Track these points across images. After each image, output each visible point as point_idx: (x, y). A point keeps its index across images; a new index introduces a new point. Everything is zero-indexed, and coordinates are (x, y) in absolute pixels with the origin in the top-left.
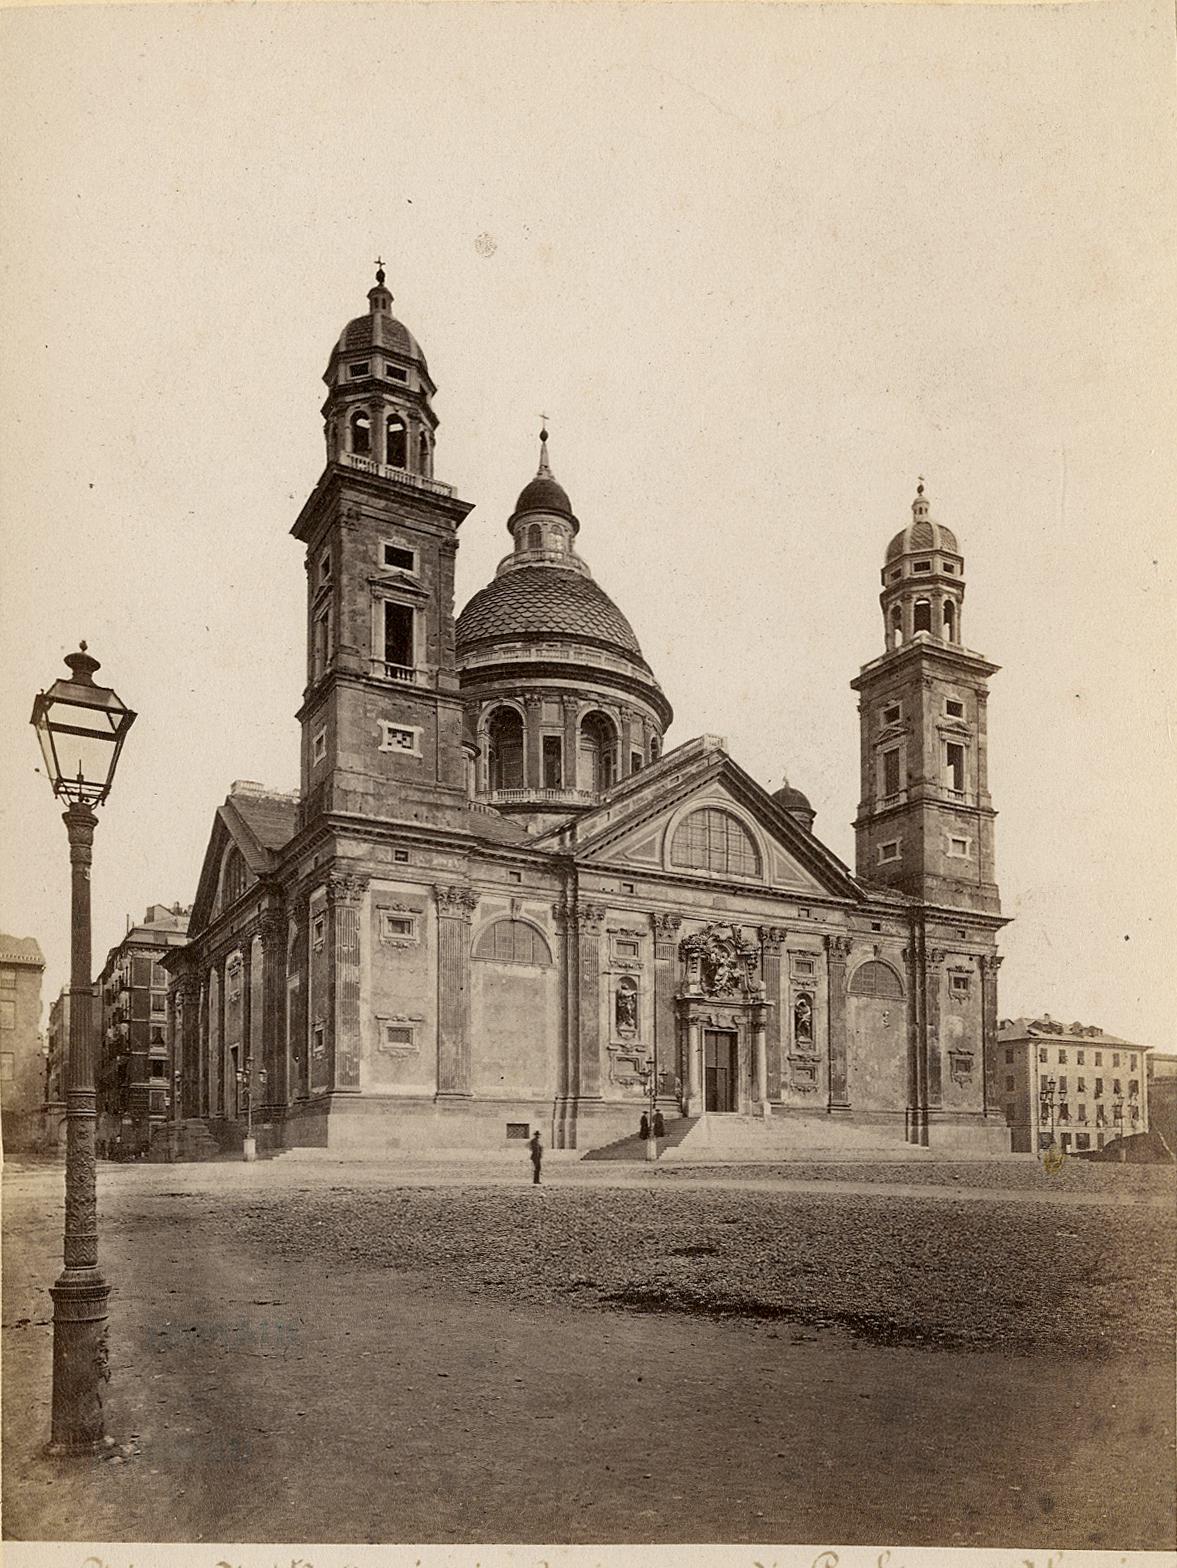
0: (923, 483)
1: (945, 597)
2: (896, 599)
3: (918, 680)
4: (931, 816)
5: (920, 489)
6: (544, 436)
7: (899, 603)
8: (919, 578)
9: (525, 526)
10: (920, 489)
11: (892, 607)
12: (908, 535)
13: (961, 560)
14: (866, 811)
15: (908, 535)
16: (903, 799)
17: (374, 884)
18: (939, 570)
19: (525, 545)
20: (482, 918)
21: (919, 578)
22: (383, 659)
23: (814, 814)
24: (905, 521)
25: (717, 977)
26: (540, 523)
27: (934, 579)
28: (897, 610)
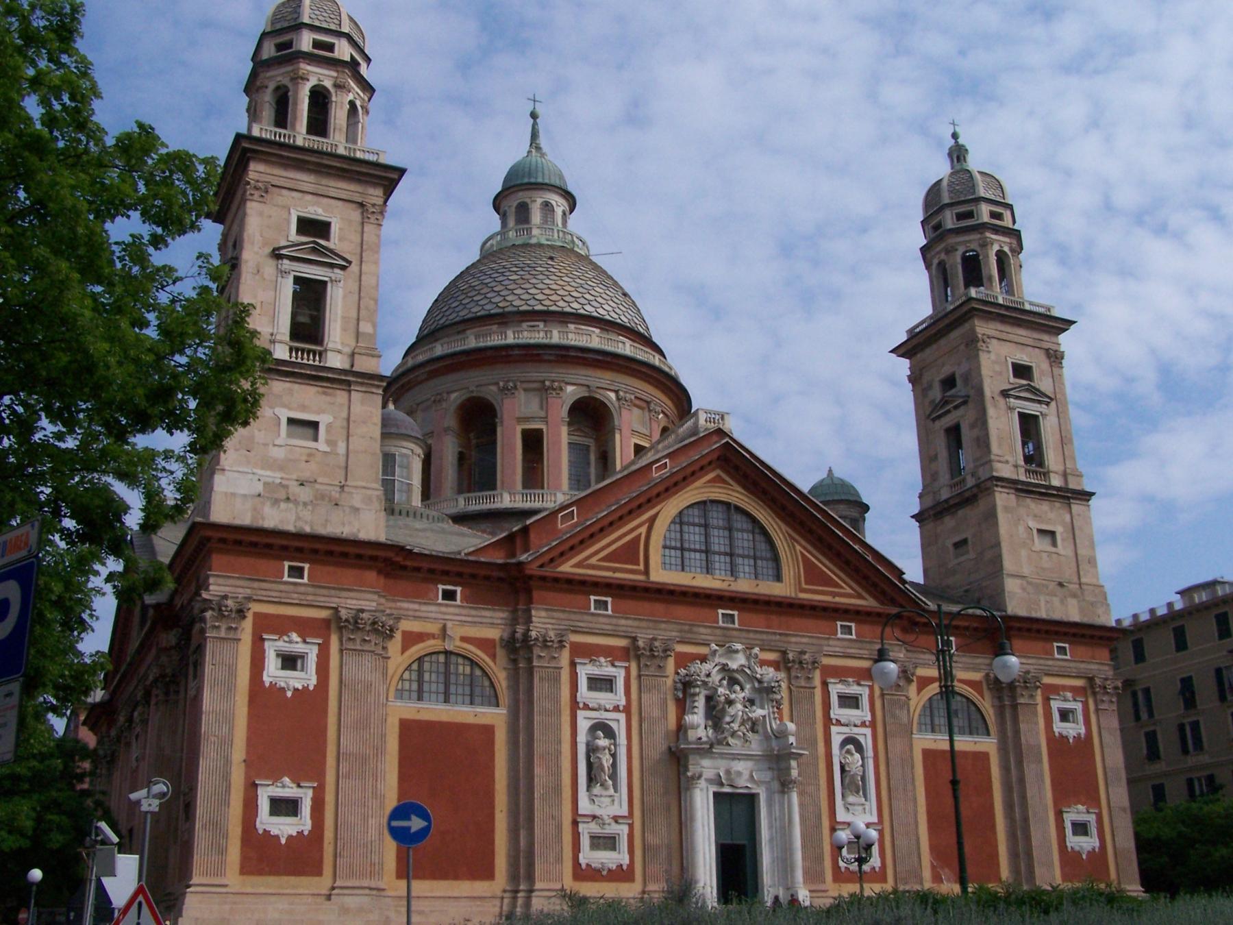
0: (958, 129)
1: (996, 247)
2: (938, 253)
3: (972, 343)
4: (1003, 499)
6: (534, 116)
7: (943, 256)
8: (965, 232)
9: (511, 204)
11: (935, 261)
12: (945, 183)
13: (1010, 207)
14: (929, 502)
15: (945, 183)
16: (970, 482)
17: (256, 608)
18: (986, 218)
19: (511, 223)
20: (404, 649)
21: (965, 232)
22: (287, 338)
23: (866, 508)
24: (941, 169)
25: (728, 719)
26: (528, 201)
27: (983, 227)
28: (942, 264)
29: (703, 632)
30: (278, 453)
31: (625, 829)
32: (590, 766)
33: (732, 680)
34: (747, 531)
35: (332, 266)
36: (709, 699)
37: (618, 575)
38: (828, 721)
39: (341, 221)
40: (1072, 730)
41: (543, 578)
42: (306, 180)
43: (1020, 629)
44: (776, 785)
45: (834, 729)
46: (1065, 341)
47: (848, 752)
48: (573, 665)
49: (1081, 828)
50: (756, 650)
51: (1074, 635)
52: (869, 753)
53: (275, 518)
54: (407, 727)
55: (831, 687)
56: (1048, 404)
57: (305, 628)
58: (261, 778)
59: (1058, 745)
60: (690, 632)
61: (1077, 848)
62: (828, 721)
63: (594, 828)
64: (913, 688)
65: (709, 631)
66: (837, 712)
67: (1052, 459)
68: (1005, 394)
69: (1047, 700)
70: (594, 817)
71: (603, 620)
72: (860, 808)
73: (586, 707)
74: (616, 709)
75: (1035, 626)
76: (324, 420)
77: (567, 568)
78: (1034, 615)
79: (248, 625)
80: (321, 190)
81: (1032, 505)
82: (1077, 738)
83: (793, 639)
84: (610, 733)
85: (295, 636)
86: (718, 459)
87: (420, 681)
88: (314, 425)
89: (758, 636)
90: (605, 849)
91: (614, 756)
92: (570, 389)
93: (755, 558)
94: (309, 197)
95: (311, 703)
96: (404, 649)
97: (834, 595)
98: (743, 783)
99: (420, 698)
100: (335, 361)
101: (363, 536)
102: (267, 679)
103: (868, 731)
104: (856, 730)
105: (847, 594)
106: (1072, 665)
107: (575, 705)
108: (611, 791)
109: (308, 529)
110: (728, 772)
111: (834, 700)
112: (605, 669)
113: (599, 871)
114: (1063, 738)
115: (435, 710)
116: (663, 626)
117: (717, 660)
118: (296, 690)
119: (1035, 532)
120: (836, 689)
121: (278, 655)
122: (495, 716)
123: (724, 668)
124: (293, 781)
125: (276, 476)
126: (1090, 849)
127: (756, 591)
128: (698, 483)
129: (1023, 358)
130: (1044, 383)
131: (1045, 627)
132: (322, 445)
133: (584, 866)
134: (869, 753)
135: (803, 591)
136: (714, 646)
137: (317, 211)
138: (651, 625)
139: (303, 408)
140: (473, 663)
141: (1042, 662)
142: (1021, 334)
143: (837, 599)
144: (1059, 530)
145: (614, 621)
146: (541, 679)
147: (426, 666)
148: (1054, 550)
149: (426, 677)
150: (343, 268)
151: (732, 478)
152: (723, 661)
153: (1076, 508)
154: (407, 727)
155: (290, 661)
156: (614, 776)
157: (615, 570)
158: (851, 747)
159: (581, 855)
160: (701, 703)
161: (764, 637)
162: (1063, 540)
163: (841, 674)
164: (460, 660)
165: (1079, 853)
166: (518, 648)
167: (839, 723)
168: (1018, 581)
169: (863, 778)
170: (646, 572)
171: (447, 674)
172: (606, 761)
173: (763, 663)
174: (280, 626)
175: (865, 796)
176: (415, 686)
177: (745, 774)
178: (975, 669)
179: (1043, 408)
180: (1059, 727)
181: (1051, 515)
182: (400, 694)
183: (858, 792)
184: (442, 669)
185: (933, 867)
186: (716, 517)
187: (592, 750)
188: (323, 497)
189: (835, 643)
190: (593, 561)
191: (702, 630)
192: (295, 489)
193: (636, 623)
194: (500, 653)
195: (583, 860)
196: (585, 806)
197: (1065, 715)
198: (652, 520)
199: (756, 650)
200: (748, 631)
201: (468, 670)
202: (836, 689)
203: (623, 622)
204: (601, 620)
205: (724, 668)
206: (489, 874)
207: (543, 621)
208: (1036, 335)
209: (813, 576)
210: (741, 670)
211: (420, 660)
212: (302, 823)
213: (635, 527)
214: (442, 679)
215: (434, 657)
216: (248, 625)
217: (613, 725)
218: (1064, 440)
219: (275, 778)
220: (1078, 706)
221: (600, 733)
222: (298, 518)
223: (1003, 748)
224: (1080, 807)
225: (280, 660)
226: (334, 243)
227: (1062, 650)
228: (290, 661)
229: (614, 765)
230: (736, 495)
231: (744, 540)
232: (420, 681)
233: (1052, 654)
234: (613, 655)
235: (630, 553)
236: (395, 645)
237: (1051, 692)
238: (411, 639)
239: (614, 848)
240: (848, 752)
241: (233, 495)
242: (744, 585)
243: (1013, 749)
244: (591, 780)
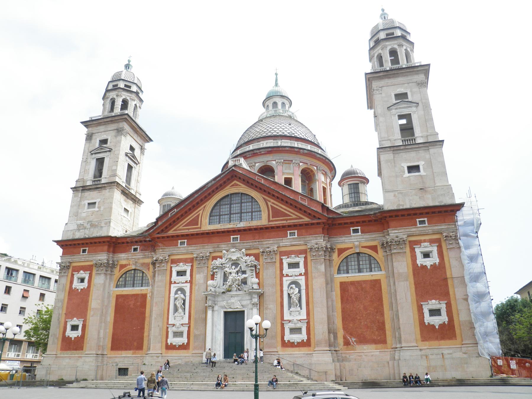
6: (276, 74)
20: (120, 271)
29: (223, 246)
30: (84, 215)
31: (187, 329)
32: (175, 305)
33: (235, 264)
34: (249, 202)
35: (106, 152)
37: (190, 231)
38: (282, 275)
39: (109, 136)
40: (428, 262)
41: (158, 238)
42: (102, 128)
43: (390, 217)
44: (250, 306)
45: (285, 279)
47: (291, 288)
48: (171, 267)
49: (435, 312)
50: (243, 250)
51: (427, 213)
52: (303, 287)
53: (78, 235)
55: (284, 261)
56: (417, 107)
57: (84, 268)
58: (69, 318)
59: (419, 272)
60: (218, 247)
61: (432, 323)
62: (282, 275)
63: (174, 329)
64: (335, 255)
65: (226, 246)
66: (286, 270)
69: (413, 250)
70: (174, 325)
71: (182, 249)
72: (298, 313)
73: (175, 283)
74: (186, 282)
75: (400, 213)
76: (97, 201)
77: (171, 232)
78: (401, 207)
79: (70, 270)
80: (106, 129)
81: (404, 155)
82: (434, 266)
83: (265, 243)
85: (82, 272)
86: (232, 177)
87: (125, 281)
88: (95, 203)
89: (248, 244)
90: (179, 337)
91: (184, 301)
92: (257, 164)
93: (252, 212)
94: (103, 133)
95: (86, 292)
96: (120, 271)
97: (287, 220)
99: (125, 287)
100: (103, 181)
101: (103, 235)
102: (74, 287)
103: (303, 278)
104: (296, 278)
105: (295, 217)
106: (428, 228)
107: (171, 283)
108: (182, 314)
109: (87, 237)
110: (227, 303)
111: (285, 266)
112: (182, 267)
113: (175, 346)
114: (424, 267)
115: (128, 290)
116: (206, 247)
117: (226, 257)
118: (81, 289)
119: (406, 169)
120: (286, 261)
121: (78, 279)
124: (78, 319)
125: (81, 222)
126: (441, 323)
127: (249, 225)
128: (228, 187)
129: (400, 90)
131: (406, 213)
133: (169, 344)
135: (272, 221)
136: (224, 251)
137: (104, 137)
138: (201, 247)
139: (93, 199)
140: (143, 273)
141: (407, 230)
142: (400, 80)
143: (289, 221)
144: (421, 164)
145: (187, 248)
146: (158, 274)
147: (128, 275)
148: (417, 174)
149: (127, 279)
150: (110, 151)
151: (242, 183)
152: (229, 257)
153: (432, 150)
155: (82, 280)
157: (188, 229)
158: (294, 286)
159: (168, 340)
161: (251, 244)
162: (424, 168)
163: (288, 254)
164: (139, 272)
165: (433, 326)
166: (154, 264)
167: (287, 275)
168: (392, 194)
170: (200, 228)
171: (134, 277)
173: (247, 255)
174: (77, 269)
175: (300, 306)
176: (123, 283)
178: (375, 240)
179: (414, 109)
180: (420, 261)
182: (117, 286)
183: (297, 306)
184: (132, 276)
185: (345, 338)
187: (176, 299)
188: (93, 225)
189: (286, 241)
190: (181, 228)
191: (223, 246)
192: (85, 225)
193: (195, 248)
194: (151, 266)
195: (169, 342)
197: (426, 255)
198: (204, 207)
199: (243, 250)
200: (244, 243)
201: (141, 275)
202: (286, 261)
203: (190, 248)
204: (183, 249)
207: (161, 254)
208: (409, 78)
209: (276, 213)
210: (238, 259)
211: (125, 273)
213: (199, 211)
214: (132, 279)
215: (130, 272)
216: (70, 270)
217: (184, 288)
218: (428, 119)
219: (72, 318)
220: (434, 249)
221: (179, 292)
222: (85, 234)
223: (388, 277)
224: (434, 301)
225: (79, 280)
226: (109, 144)
227: (422, 222)
229: (184, 304)
230: (243, 189)
231: (247, 206)
232: (125, 281)
233: (416, 225)
234: (185, 261)
235: (195, 222)
237: (413, 244)
238: (122, 266)
239: (182, 337)
240: (291, 288)
241: (68, 231)
242: (242, 225)
243: (391, 274)
244: (176, 310)
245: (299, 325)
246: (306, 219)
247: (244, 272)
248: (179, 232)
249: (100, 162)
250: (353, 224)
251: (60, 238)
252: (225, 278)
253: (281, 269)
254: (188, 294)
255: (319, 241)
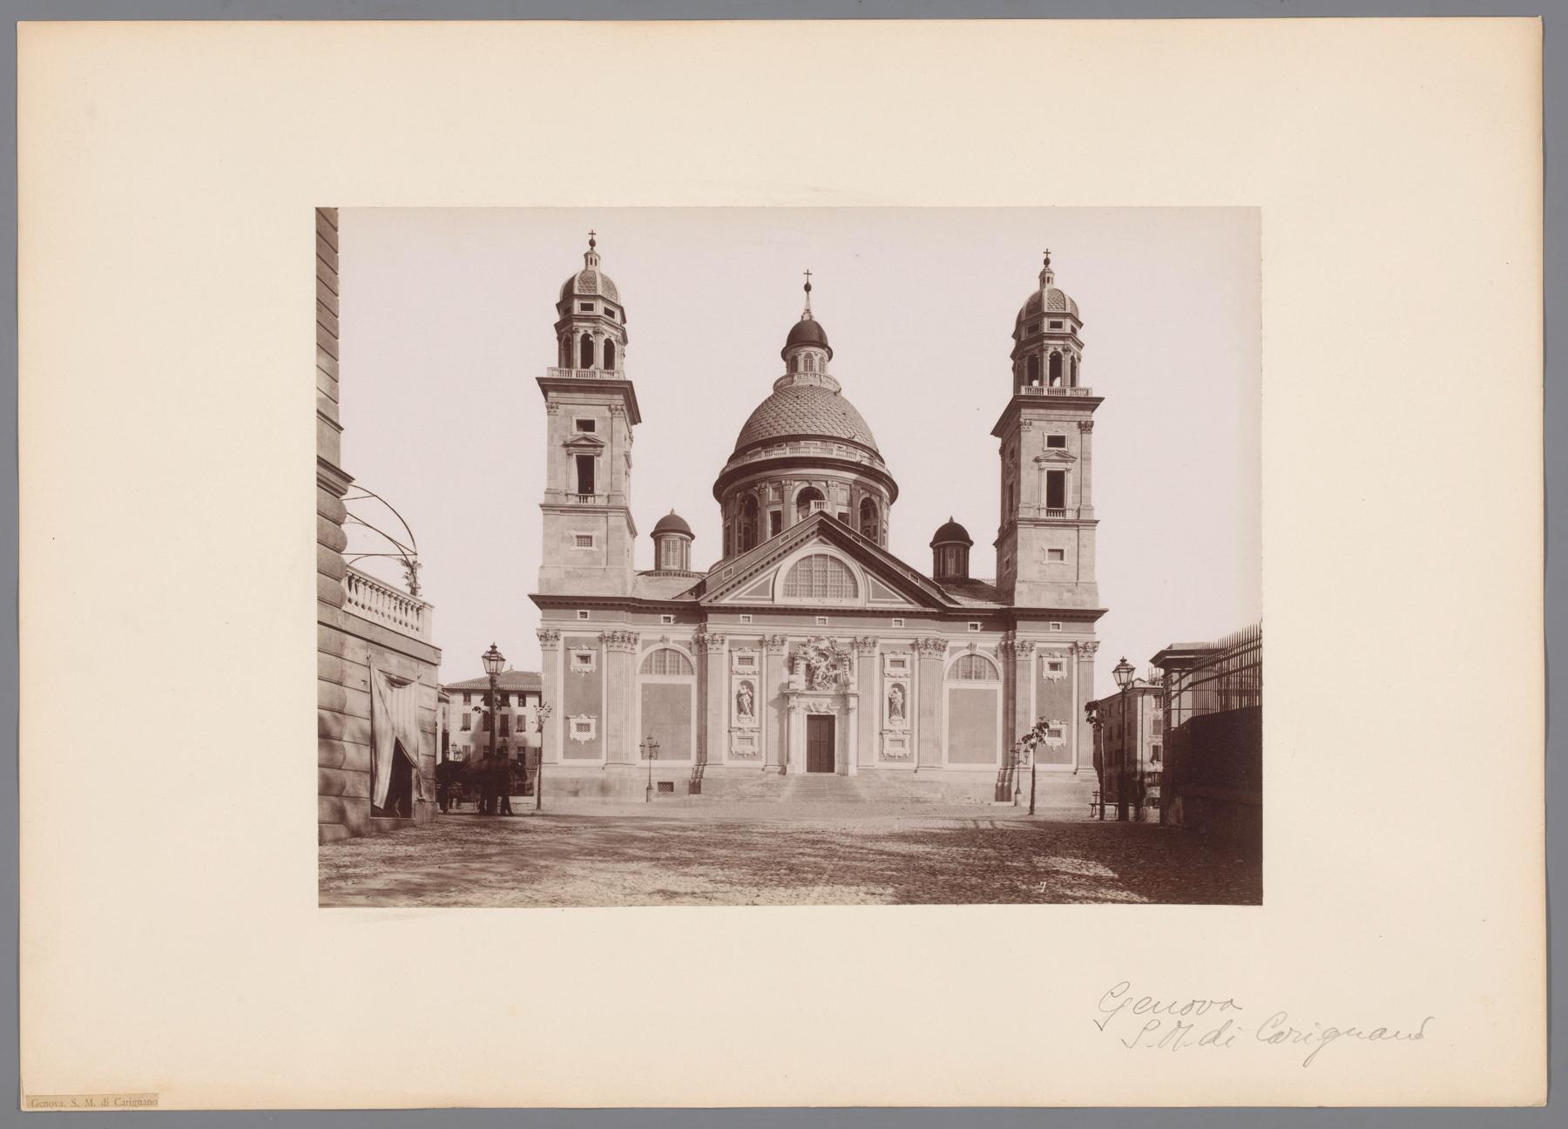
5: (1047, 262)
10: (1047, 262)
32: (739, 704)
36: (808, 666)
46: (1097, 416)
54: (645, 687)
67: (1070, 498)
68: (1037, 460)
76: (594, 534)
77: (726, 601)
84: (750, 687)
98: (823, 711)
111: (888, 662)
122: (692, 681)
123: (817, 649)
130: (1072, 447)
132: (594, 548)
134: (908, 692)
154: (645, 687)
156: (752, 710)
160: (802, 667)
166: (701, 644)
169: (903, 706)
172: (746, 700)
177: (825, 706)
179: (1069, 465)
181: (1064, 538)
186: (817, 565)
194: (695, 648)
196: (735, 724)
202: (888, 658)
205: (817, 649)
206: (689, 758)
212: (592, 734)
213: (768, 574)
218: (1083, 486)
228: (585, 659)
236: (638, 647)
238: (646, 644)
245: (901, 736)
246: (915, 607)
247: (834, 667)
248: (736, 603)
249: (586, 469)
250: (972, 618)
251: (536, 592)
252: (811, 671)
253: (883, 666)
254: (757, 689)
255: (929, 631)
